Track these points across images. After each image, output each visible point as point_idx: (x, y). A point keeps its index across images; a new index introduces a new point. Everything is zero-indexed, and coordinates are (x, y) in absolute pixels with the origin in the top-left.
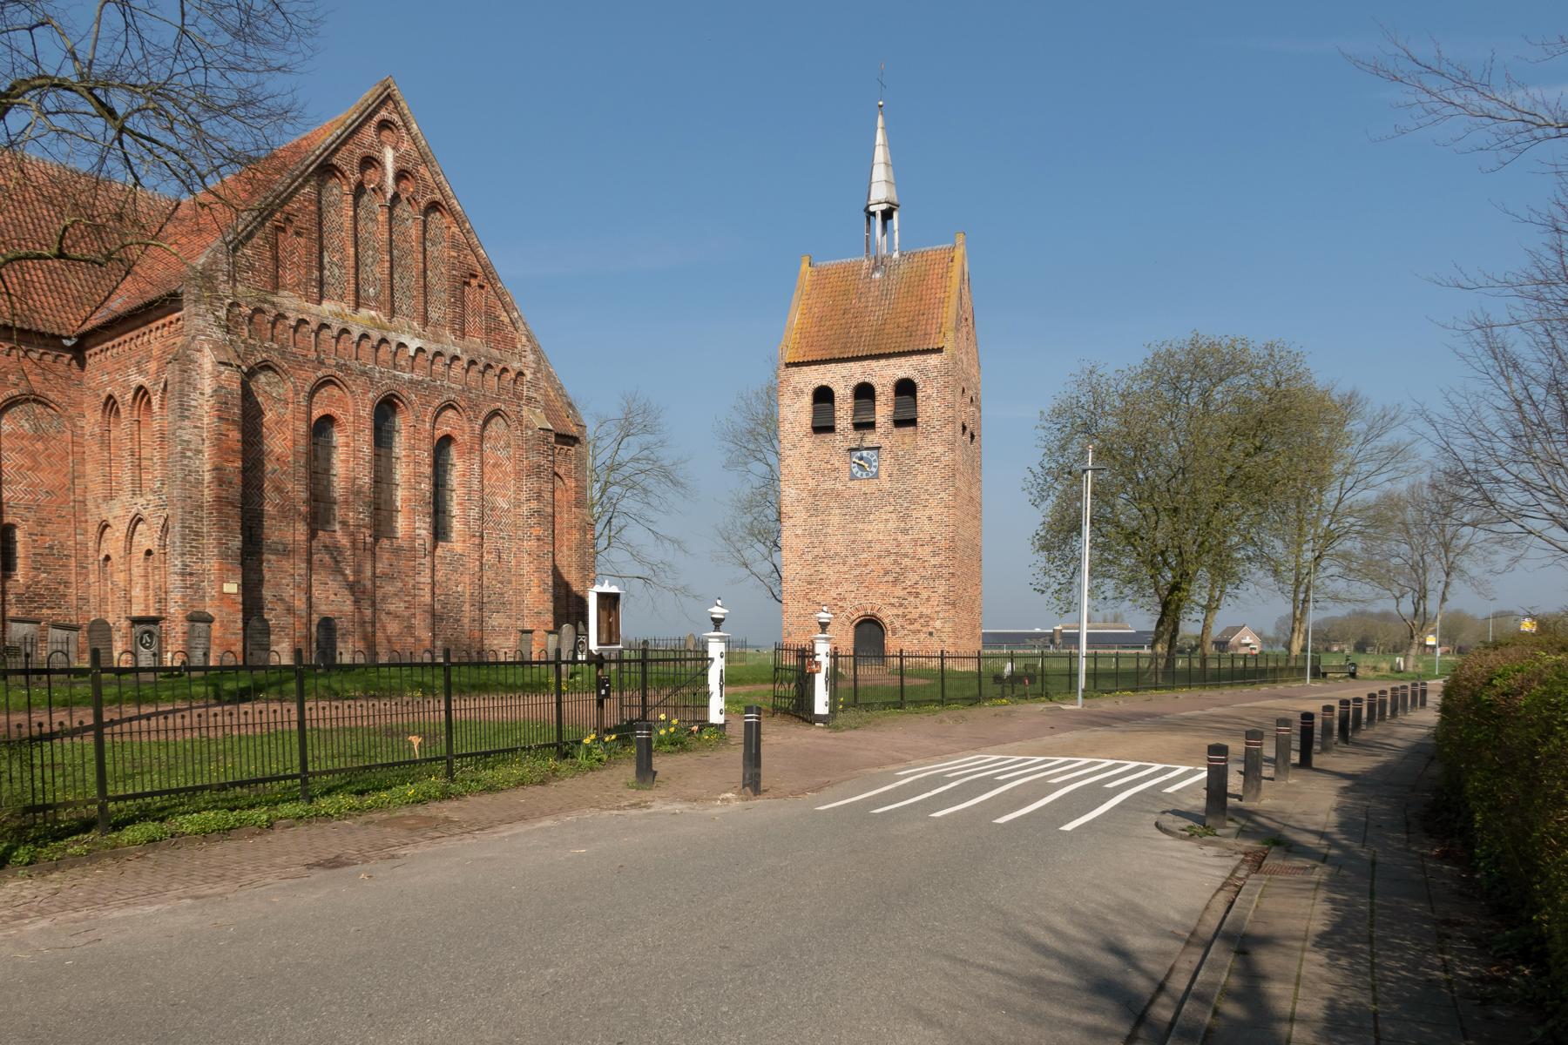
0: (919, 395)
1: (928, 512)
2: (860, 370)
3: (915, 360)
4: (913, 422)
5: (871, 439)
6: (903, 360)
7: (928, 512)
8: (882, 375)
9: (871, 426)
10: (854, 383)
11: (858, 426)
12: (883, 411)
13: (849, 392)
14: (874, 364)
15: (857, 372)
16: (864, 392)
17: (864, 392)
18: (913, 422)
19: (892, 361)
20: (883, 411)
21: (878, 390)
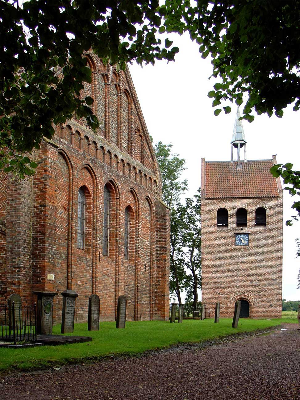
0: (267, 214)
1: (271, 259)
2: (240, 203)
3: (265, 200)
4: (264, 224)
5: (245, 230)
6: (260, 200)
7: (271, 259)
8: (251, 207)
9: (245, 225)
10: (237, 208)
11: (238, 225)
12: (251, 220)
13: (235, 211)
14: (247, 201)
15: (240, 204)
16: (242, 214)
17: (242, 214)
18: (264, 224)
19: (255, 200)
20: (251, 220)
21: (248, 212)
